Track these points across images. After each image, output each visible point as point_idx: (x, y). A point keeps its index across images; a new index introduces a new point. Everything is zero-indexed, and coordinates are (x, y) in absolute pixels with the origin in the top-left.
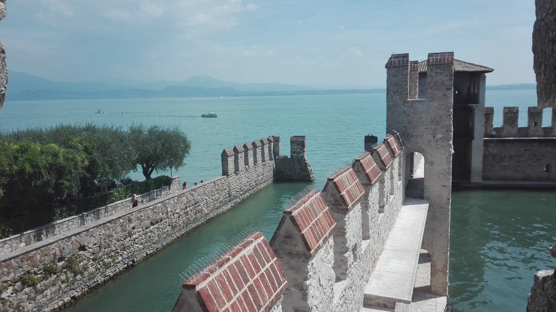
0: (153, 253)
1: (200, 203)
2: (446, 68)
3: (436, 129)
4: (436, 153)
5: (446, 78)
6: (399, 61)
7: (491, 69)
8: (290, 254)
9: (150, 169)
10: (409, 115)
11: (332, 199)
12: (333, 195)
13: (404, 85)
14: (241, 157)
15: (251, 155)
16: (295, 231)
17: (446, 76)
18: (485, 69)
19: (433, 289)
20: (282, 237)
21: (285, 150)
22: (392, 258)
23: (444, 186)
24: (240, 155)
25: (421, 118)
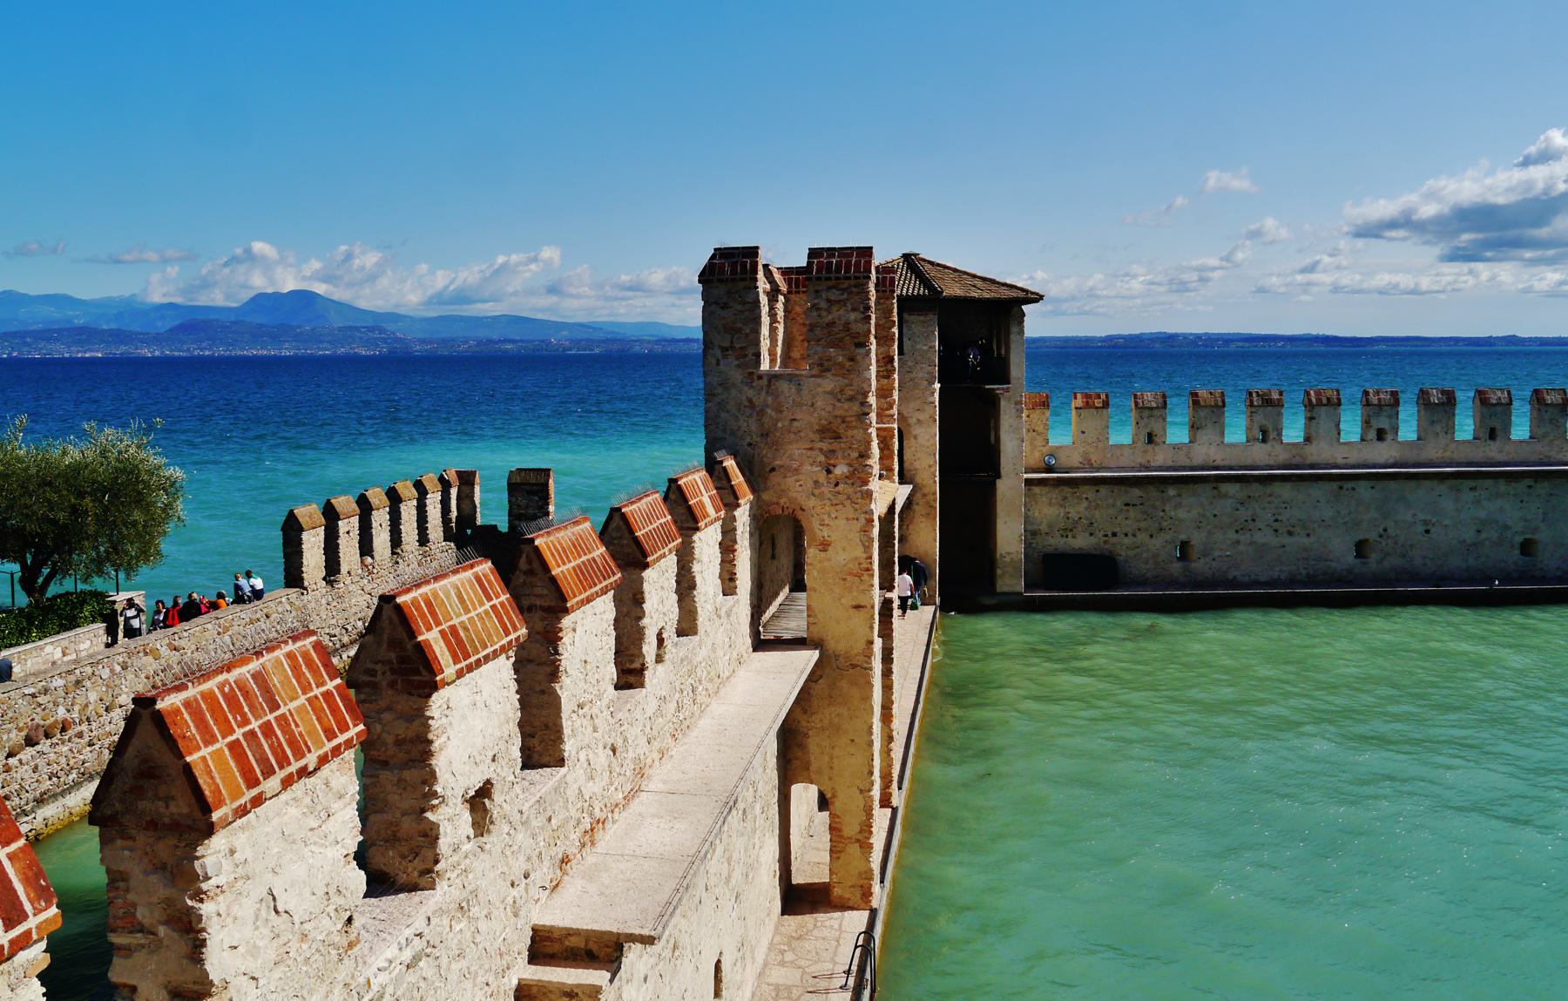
0: (30, 834)
2: (853, 289)
3: (833, 451)
4: (833, 516)
5: (853, 316)
7: (1037, 294)
9: (46, 571)
10: (762, 413)
11: (393, 655)
12: (394, 644)
13: (748, 331)
14: (348, 533)
16: (167, 758)
17: (854, 310)
18: (1021, 294)
19: (837, 891)
20: (130, 775)
22: (654, 816)
23: (858, 607)
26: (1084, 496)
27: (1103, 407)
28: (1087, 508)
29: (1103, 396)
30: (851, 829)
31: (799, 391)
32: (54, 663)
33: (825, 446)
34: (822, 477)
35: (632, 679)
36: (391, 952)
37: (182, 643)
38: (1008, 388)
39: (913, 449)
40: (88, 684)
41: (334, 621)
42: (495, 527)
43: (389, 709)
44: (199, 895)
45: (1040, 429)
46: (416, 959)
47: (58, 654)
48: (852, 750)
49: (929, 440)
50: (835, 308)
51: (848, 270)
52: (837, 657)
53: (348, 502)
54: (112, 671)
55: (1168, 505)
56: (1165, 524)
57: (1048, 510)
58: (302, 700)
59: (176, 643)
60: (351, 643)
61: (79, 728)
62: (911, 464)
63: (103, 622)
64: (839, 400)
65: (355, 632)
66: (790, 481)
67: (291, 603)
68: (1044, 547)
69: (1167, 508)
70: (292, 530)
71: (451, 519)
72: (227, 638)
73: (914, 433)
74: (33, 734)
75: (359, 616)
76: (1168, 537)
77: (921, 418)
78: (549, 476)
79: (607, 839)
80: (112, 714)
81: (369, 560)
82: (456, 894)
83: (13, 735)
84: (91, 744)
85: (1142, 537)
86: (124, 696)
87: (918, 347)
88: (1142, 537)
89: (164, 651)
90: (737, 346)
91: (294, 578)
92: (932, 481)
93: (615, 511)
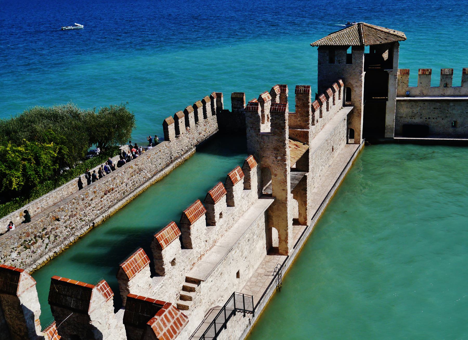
1: (144, 171)
2: (282, 115)
3: (277, 154)
5: (281, 122)
7: (404, 38)
8: (123, 279)
10: (260, 143)
12: (156, 243)
14: (182, 122)
17: (281, 120)
19: (280, 251)
21: (227, 105)
22: (215, 252)
23: (283, 190)
26: (419, 105)
27: (429, 74)
28: (420, 109)
29: (429, 70)
30: (283, 238)
31: (269, 139)
33: (275, 152)
34: (275, 159)
35: (213, 224)
36: (157, 287)
38: (392, 71)
39: (354, 95)
40: (116, 178)
41: (179, 149)
42: (228, 110)
43: (156, 252)
44: (129, 287)
45: (405, 82)
46: (162, 287)
48: (283, 221)
49: (359, 92)
50: (277, 120)
51: (280, 111)
52: (279, 200)
53: (181, 113)
54: (122, 174)
55: (450, 109)
56: (448, 115)
57: (405, 110)
58: (141, 260)
59: (137, 164)
60: (184, 154)
61: (116, 189)
62: (353, 100)
63: (119, 155)
64: (278, 142)
65: (185, 150)
66: (267, 160)
67: (166, 146)
68: (404, 122)
69: (449, 110)
70: (165, 125)
71: (214, 109)
72: (150, 160)
73: (355, 90)
74: (106, 192)
75: (186, 145)
76: (449, 120)
78: (243, 95)
79: (204, 258)
80: (123, 185)
81: (189, 128)
82: (169, 276)
83: (101, 193)
84: (119, 193)
85: (439, 119)
86: (125, 180)
87: (357, 61)
88: (439, 119)
89: (134, 166)
90: (254, 127)
91: (166, 138)
92: (360, 106)
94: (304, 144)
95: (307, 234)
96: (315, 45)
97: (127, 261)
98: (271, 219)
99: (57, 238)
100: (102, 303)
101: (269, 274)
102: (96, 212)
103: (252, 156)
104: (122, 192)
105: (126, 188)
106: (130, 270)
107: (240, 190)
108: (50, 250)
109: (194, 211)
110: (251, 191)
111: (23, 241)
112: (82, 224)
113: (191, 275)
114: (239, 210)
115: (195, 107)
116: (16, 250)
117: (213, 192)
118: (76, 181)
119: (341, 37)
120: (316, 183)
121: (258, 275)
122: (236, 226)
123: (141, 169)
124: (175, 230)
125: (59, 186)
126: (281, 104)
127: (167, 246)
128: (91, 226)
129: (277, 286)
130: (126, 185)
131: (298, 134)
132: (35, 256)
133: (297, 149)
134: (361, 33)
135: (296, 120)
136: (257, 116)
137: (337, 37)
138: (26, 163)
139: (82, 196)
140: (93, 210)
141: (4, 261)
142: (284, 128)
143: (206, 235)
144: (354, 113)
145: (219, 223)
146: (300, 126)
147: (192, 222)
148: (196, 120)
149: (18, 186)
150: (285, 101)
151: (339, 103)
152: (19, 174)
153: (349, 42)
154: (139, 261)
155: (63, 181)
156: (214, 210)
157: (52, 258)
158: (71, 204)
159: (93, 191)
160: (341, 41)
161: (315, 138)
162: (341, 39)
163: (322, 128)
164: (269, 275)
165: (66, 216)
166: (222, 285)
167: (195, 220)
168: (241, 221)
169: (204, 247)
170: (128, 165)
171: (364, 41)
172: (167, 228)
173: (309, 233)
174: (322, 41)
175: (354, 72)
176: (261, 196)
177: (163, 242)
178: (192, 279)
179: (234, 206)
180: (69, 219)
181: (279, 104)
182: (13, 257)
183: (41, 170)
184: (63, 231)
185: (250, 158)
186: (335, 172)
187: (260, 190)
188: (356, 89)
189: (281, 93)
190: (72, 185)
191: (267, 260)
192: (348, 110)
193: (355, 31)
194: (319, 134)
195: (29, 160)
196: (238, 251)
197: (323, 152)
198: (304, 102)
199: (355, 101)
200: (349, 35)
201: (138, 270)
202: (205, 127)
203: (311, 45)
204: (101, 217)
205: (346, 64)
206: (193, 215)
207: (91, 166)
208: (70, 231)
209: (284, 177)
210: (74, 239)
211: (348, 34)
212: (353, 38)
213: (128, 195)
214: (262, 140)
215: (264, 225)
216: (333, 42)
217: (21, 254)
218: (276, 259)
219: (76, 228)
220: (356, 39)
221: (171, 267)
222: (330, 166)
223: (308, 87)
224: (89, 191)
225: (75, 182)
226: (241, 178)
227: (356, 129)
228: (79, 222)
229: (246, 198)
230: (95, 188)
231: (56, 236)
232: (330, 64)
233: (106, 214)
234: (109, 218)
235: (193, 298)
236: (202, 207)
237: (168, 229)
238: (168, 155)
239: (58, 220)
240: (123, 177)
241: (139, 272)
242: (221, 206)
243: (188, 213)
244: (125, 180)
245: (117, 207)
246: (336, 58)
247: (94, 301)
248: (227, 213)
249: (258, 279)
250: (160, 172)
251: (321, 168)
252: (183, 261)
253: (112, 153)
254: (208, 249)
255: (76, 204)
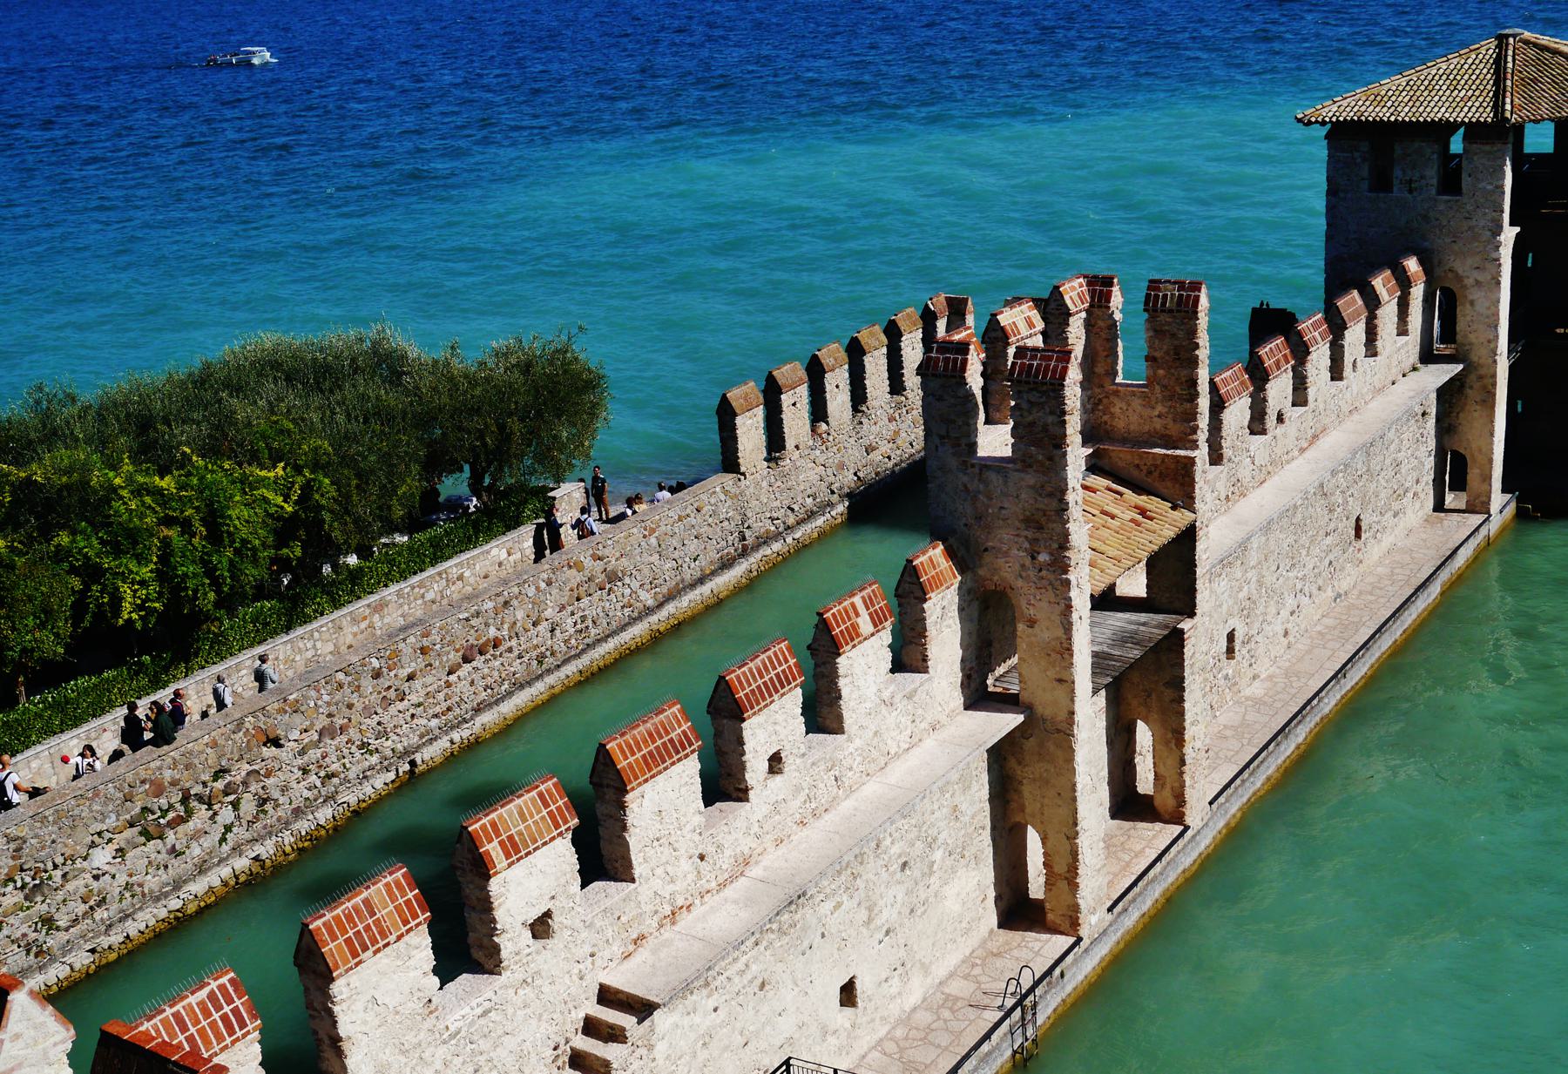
1: (627, 580)
3: (1037, 540)
5: (1050, 419)
6: (946, 360)
10: (975, 499)
12: (470, 851)
14: (794, 404)
15: (837, 387)
17: (1052, 413)
19: (1050, 916)
22: (736, 902)
23: (1060, 681)
24: (786, 399)
25: (1002, 508)
31: (1006, 482)
32: (500, 564)
33: (1029, 534)
34: (1028, 561)
35: (741, 795)
36: (467, 1010)
37: (607, 552)
39: (1468, 318)
40: (515, 602)
41: (777, 503)
43: (472, 882)
44: (332, 1002)
46: (485, 1013)
47: (504, 554)
48: (1060, 803)
49: (1489, 308)
50: (1035, 411)
52: (1044, 720)
53: (794, 370)
54: (538, 588)
58: (391, 907)
61: (509, 644)
62: (1465, 336)
65: (802, 511)
66: (1001, 561)
67: (726, 493)
70: (726, 415)
72: (653, 541)
73: (1471, 297)
74: (468, 653)
75: (809, 492)
77: (1479, 278)
79: (685, 920)
80: (540, 628)
81: (824, 426)
82: (520, 976)
83: (451, 656)
84: (520, 657)
89: (588, 562)
91: (730, 463)
92: (1490, 361)
93: (722, 678)
94: (1174, 508)
95: (1186, 858)
96: (1313, 119)
97: (336, 908)
98: (1018, 791)
99: (268, 807)
100: (55, 1044)
101: (986, 1001)
102: (424, 721)
103: (941, 547)
104: (534, 654)
105: (549, 642)
106: (341, 940)
107: (872, 671)
108: (237, 850)
109: (645, 741)
110: (930, 679)
111: (138, 810)
112: (367, 764)
113: (622, 979)
114: (865, 747)
115: (856, 352)
116: (110, 840)
117: (744, 673)
118: (369, 606)
119: (1422, 88)
120: (1267, 660)
121: (946, 1000)
122: (847, 806)
123: (614, 573)
124: (553, 807)
125: (307, 620)
126: (1053, 351)
127: (513, 863)
128: (401, 774)
129: (1015, 1052)
130: (552, 631)
131: (1156, 466)
132: (178, 867)
133: (1138, 524)
134: (1505, 73)
135: (1147, 412)
136: (961, 393)
137: (1408, 88)
138: (172, 533)
139: (376, 663)
140: (413, 716)
141: (64, 876)
142: (1059, 442)
143: (700, 834)
144: (1469, 392)
145: (765, 793)
146: (1163, 437)
147: (630, 782)
148: (858, 396)
149: (142, 613)
150: (1108, 340)
151: (1399, 348)
152: (146, 572)
153: (1450, 110)
154: (383, 912)
155: (319, 604)
156: (741, 742)
157: (242, 879)
158: (329, 687)
159: (419, 645)
160: (1418, 104)
161: (1265, 485)
162: (1422, 99)
163: (1305, 445)
164: (985, 1008)
165: (306, 731)
166: (768, 1028)
167: (648, 775)
168: (872, 789)
169: (691, 877)
170: (564, 557)
171: (1508, 107)
172: (519, 797)
173: (1195, 855)
174: (1345, 103)
175: (1470, 228)
176: (977, 697)
177: (494, 848)
178: (620, 996)
179: (843, 733)
180: (320, 741)
181: (1043, 350)
182: (96, 864)
183: (225, 560)
184: (294, 784)
185: (931, 553)
186: (1356, 619)
187: (975, 676)
188: (1475, 294)
189: (1091, 306)
190: (355, 621)
191: (993, 946)
192: (1442, 373)
193: (1482, 66)
194: (1287, 467)
195: (186, 526)
196: (848, 904)
197: (1304, 540)
198: (1176, 342)
199: (1471, 344)
200: (1455, 83)
201: (374, 941)
202: (893, 426)
203: (1299, 120)
204: (443, 744)
205: (1439, 193)
206: (638, 755)
207: (435, 554)
208: (318, 784)
209: (1060, 633)
210: (334, 817)
211: (1451, 77)
212: (1470, 93)
213: (559, 666)
214: (981, 486)
215: (988, 813)
216: (1385, 109)
217: (130, 855)
218: (1030, 945)
219: (342, 776)
220: (1481, 99)
221: (531, 941)
222: (1339, 595)
223: (1196, 286)
224: (401, 645)
225: (368, 611)
226: (875, 625)
227: (1473, 456)
228: (358, 754)
229: (905, 702)
230: (426, 635)
231: (265, 801)
232: (1373, 195)
233: (466, 734)
234: (473, 746)
235: (614, 1066)
236: (684, 727)
237: (526, 800)
238: (732, 527)
239: (276, 742)
240: (542, 598)
241: (378, 950)
242: (777, 728)
243: (619, 746)
244: (548, 613)
245: (508, 708)
246: (1397, 173)
247: (17, 1036)
248: (804, 755)
249: (939, 1019)
250: (693, 586)
251: (1290, 602)
252: (589, 926)
253: (517, 509)
254: (708, 887)
255: (347, 690)
